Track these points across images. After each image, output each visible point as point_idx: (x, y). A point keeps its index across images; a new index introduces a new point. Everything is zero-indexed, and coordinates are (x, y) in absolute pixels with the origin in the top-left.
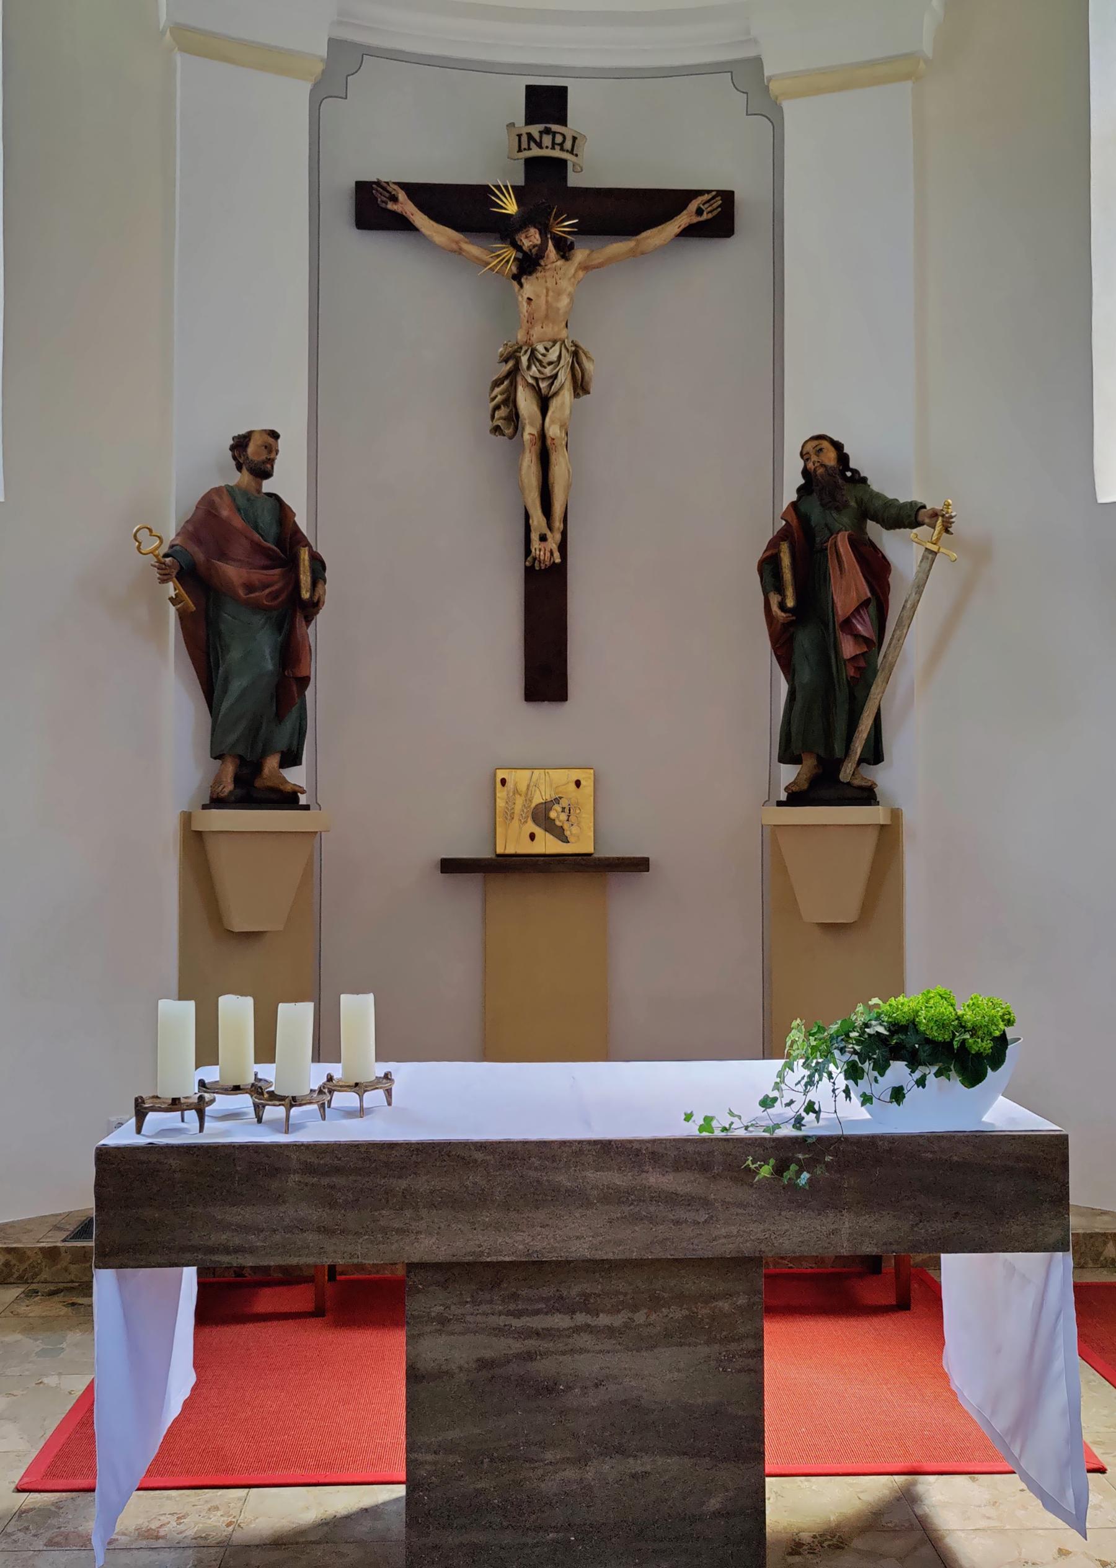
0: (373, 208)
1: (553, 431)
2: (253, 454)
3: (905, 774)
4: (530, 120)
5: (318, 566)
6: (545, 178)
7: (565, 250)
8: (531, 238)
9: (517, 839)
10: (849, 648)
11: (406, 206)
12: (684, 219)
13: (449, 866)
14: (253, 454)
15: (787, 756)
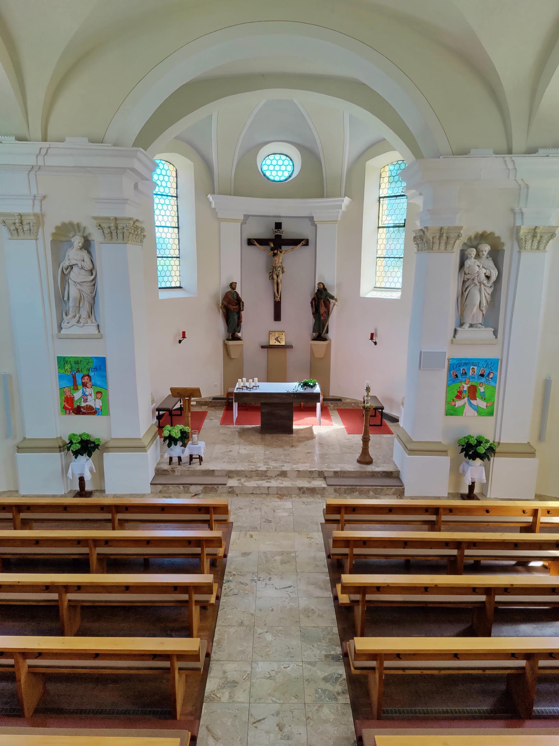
0: (250, 242)
1: (279, 281)
2: (233, 286)
3: (332, 335)
4: (276, 229)
5: (243, 303)
6: (278, 237)
7: (281, 252)
8: (276, 251)
9: (273, 342)
10: (322, 318)
11: (256, 243)
12: (301, 244)
13: (263, 347)
14: (233, 286)
15: (313, 332)
